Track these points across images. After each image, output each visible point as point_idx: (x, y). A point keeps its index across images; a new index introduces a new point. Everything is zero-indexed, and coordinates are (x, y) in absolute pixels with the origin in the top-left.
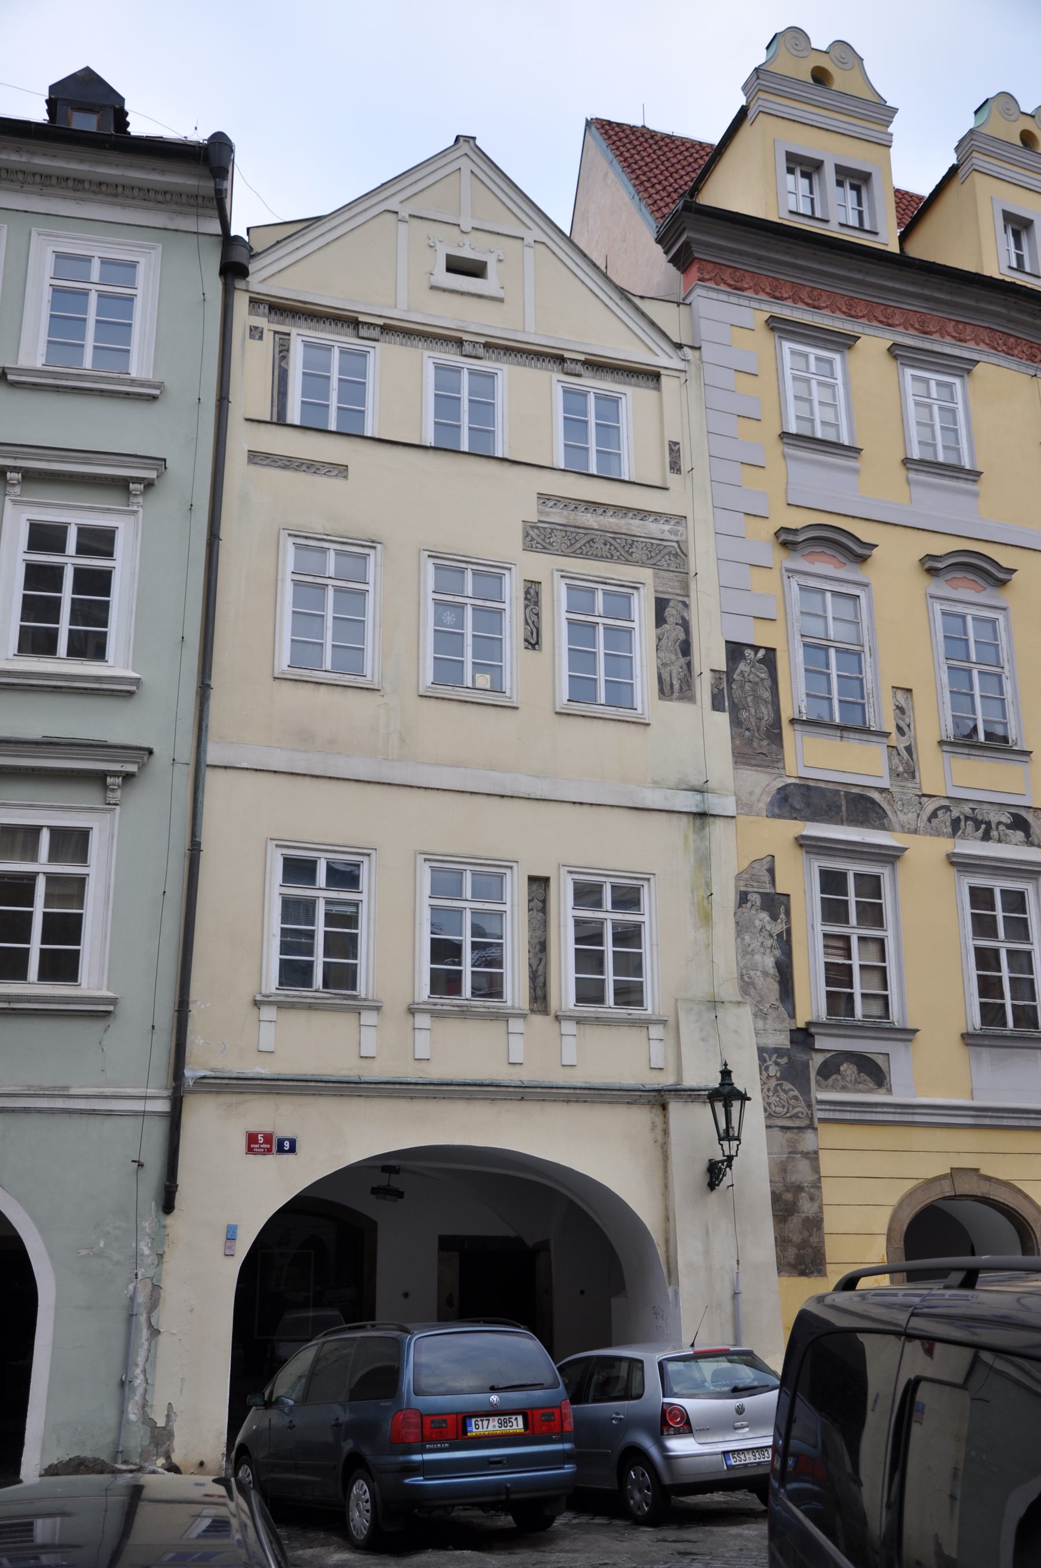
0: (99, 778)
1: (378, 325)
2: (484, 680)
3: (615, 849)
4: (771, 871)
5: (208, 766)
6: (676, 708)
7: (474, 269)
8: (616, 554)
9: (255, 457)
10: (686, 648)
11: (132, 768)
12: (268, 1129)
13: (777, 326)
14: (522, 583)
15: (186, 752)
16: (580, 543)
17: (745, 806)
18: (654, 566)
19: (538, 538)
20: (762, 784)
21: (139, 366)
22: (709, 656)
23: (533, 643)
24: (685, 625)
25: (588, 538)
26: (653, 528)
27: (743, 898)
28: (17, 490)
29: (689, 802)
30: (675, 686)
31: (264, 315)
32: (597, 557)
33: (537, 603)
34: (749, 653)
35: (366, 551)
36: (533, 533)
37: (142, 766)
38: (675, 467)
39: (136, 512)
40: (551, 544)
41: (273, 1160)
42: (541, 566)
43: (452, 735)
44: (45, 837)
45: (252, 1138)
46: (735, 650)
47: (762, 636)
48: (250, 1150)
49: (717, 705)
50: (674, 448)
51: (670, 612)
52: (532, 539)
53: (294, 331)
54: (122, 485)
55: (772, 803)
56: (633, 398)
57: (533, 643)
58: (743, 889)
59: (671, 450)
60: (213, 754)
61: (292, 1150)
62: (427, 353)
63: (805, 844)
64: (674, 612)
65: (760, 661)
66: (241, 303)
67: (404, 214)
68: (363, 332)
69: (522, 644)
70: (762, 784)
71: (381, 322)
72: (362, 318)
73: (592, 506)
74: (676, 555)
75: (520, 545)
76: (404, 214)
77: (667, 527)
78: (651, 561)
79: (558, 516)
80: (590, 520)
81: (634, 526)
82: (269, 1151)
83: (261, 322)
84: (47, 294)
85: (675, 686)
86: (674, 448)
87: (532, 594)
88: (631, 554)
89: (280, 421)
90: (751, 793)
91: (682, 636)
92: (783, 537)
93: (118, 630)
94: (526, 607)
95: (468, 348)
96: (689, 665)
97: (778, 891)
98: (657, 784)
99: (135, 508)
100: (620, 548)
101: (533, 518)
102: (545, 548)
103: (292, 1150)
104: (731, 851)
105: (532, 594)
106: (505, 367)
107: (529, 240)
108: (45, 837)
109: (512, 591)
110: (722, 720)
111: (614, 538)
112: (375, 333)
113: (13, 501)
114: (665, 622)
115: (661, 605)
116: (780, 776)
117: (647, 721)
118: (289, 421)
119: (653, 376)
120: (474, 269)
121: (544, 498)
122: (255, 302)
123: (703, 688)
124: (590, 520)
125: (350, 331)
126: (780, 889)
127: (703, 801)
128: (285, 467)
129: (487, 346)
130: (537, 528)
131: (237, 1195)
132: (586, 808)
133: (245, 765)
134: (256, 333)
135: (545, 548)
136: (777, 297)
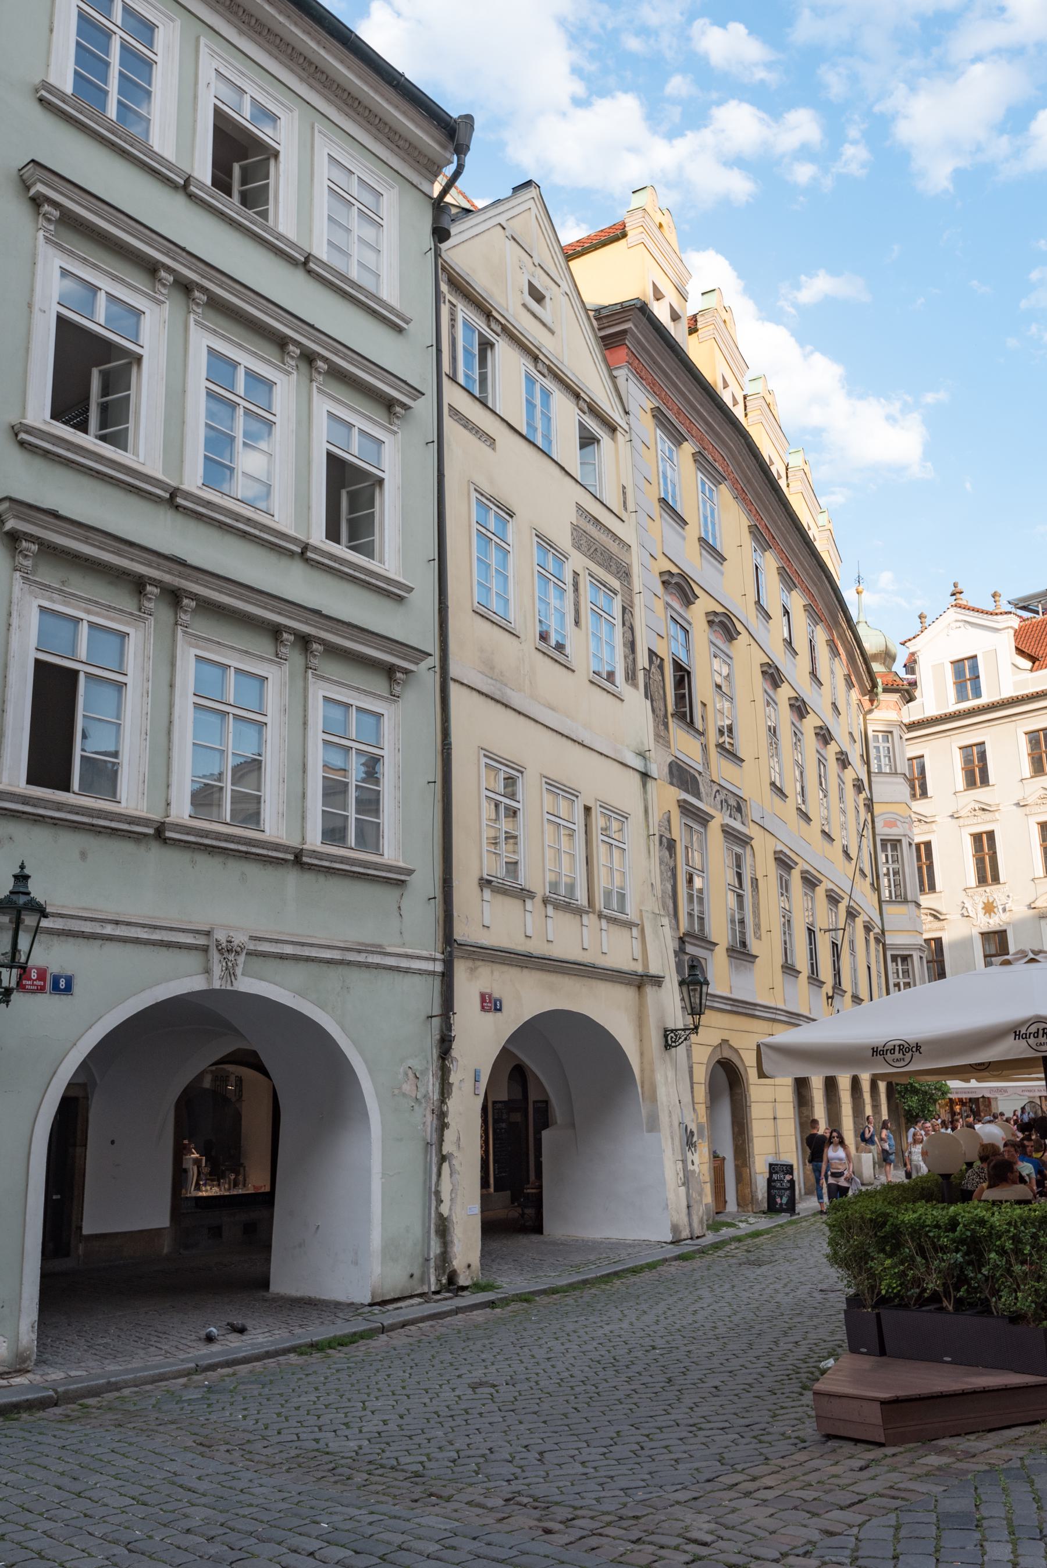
0: (390, 672)
1: (501, 323)
5: (452, 679)
12: (488, 991)
21: (389, 292)
23: (577, 623)
28: (321, 378)
35: (507, 517)
36: (575, 533)
39: (396, 433)
41: (490, 1017)
42: (577, 561)
45: (483, 997)
48: (483, 1008)
54: (389, 405)
57: (577, 623)
61: (500, 1010)
62: (523, 361)
68: (494, 325)
72: (495, 313)
82: (489, 1011)
85: (631, 677)
92: (666, 578)
95: (540, 366)
96: (634, 660)
99: (395, 429)
103: (500, 1010)
109: (569, 578)
110: (649, 702)
112: (498, 329)
113: (318, 388)
125: (484, 319)
128: (465, 427)
131: (480, 1041)
133: (465, 682)
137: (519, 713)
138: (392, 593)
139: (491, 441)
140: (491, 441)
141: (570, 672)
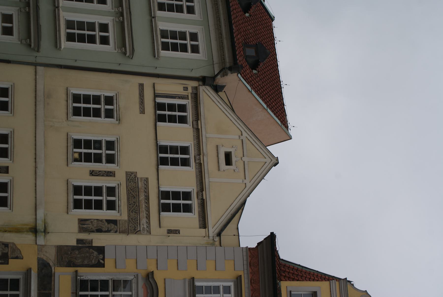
2: (76, 156)
3: (20, 196)
4: (17, 258)
6: (75, 226)
7: (228, 161)
8: (131, 206)
9: (141, 86)
10: (99, 231)
11: (33, 45)
13: (238, 280)
14: (114, 170)
15: (39, 60)
16: (133, 193)
17: (41, 248)
18: (129, 221)
19: (131, 177)
20: (51, 256)
22: (99, 240)
23: (93, 173)
24: (108, 231)
25: (135, 196)
26: (144, 221)
27: (6, 245)
29: (40, 226)
30: (83, 225)
31: (192, 91)
32: (128, 199)
33: (107, 176)
34: (101, 256)
37: (33, 49)
38: (170, 232)
40: (130, 182)
43: (56, 148)
44: (10, 25)
46: (101, 250)
47: (109, 262)
49: (79, 241)
50: (177, 232)
51: (113, 226)
52: (131, 175)
53: (190, 101)
55: (43, 260)
56: (193, 218)
57: (93, 173)
58: (9, 245)
59: (176, 230)
60: (39, 68)
62: (192, 143)
63: (28, 272)
64: (113, 227)
65: (99, 261)
66: (195, 84)
67: (242, 138)
69: (92, 169)
70: (51, 256)
71: (200, 127)
73: (147, 198)
74: (135, 230)
75: (128, 170)
76: (242, 138)
77: (145, 227)
78: (131, 220)
79: (141, 185)
80: (142, 197)
81: (143, 214)
83: (190, 90)
84: (183, 30)
85: (83, 225)
86: (177, 232)
87: (110, 174)
88: (132, 212)
89: (156, 96)
90: (46, 252)
91: (104, 229)
93: (76, 45)
94: (105, 172)
95: (198, 157)
96: (93, 232)
97: (10, 260)
98: (45, 215)
99: (117, 50)
100: (134, 207)
101: (139, 176)
102: (128, 180)
104: (23, 241)
105: (110, 174)
106: (194, 169)
107: (245, 181)
108: (10, 25)
111: (137, 206)
114: (108, 224)
115: (114, 222)
116: (54, 265)
117: (69, 213)
118: (156, 98)
119: (204, 224)
120: (228, 161)
121: (147, 180)
122: (196, 88)
123: (84, 236)
124: (142, 197)
126: (10, 260)
127: (41, 232)
129: (200, 164)
130: (135, 177)
132: (34, 188)
133: (37, 77)
134: (186, 89)
135: (128, 180)
136: (252, 282)
137: (36, 115)
138: (57, 44)
139: (142, 111)
140: (142, 111)
141: (66, 163)
